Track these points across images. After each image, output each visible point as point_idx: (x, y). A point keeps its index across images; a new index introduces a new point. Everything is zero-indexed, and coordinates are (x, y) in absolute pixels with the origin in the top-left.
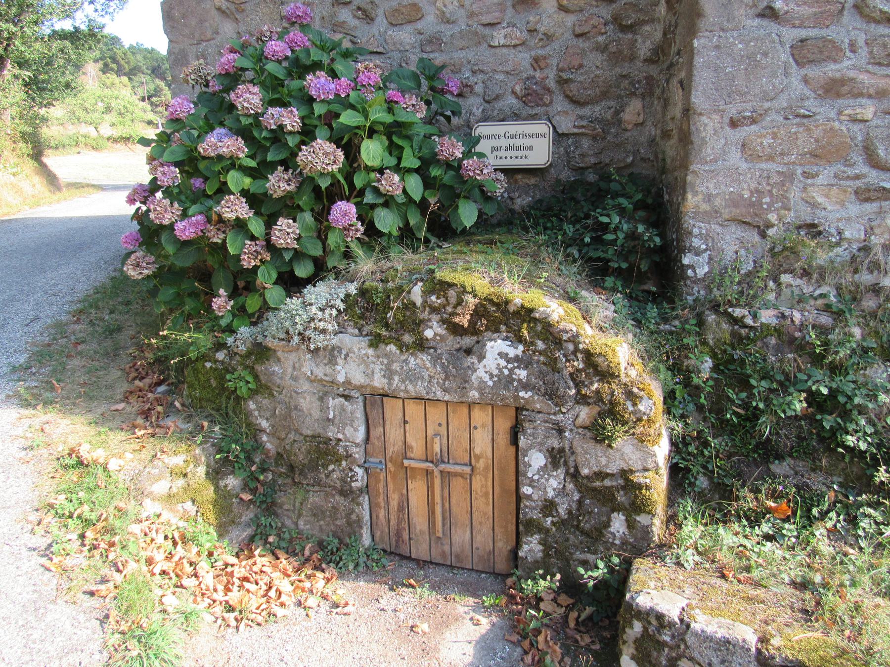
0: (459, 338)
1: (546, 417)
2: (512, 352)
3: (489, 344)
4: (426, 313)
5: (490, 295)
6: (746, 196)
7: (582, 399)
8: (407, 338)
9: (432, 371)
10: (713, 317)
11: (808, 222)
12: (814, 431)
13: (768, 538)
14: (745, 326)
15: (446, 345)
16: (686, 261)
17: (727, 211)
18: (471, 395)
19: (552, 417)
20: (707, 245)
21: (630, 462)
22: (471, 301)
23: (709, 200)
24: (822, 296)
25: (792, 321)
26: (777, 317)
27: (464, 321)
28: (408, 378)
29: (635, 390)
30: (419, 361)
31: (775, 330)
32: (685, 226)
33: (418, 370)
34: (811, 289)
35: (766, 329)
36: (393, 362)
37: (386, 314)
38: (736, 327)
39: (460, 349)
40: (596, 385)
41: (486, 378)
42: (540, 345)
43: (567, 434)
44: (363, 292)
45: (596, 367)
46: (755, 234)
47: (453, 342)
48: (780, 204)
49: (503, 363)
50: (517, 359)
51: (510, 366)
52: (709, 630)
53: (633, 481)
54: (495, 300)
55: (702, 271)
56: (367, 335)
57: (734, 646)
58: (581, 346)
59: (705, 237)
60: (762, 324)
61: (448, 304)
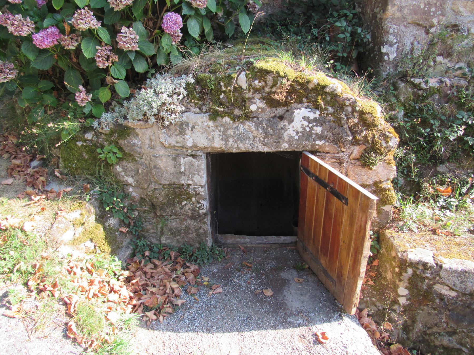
0: (274, 109)
1: (332, 155)
2: (312, 116)
3: (296, 112)
4: (251, 93)
5: (297, 78)
6: (422, 7)
7: (355, 142)
8: (237, 112)
9: (255, 133)
10: (403, 84)
11: (453, 23)
12: (460, 147)
13: (442, 208)
14: (421, 89)
15: (265, 114)
16: (384, 50)
17: (410, 17)
18: (283, 146)
19: (337, 155)
20: (397, 39)
21: (381, 177)
22: (286, 83)
23: (401, 10)
24: (460, 68)
25: (446, 84)
26: (438, 82)
27: (280, 97)
28: (239, 139)
29: (387, 134)
30: (246, 127)
31: (437, 90)
32: (385, 27)
33: (246, 133)
34: (453, 65)
35: (432, 92)
36: (228, 129)
37: (219, 95)
38: (416, 90)
39: (275, 116)
40: (364, 133)
41: (294, 134)
42: (330, 110)
43: (344, 164)
44: (198, 81)
45: (366, 121)
46: (423, 32)
47: (270, 112)
48: (440, 12)
49: (306, 123)
50: (315, 120)
51: (310, 125)
52: (454, 267)
53: (381, 187)
54: (301, 81)
55: (392, 57)
56: (206, 112)
57: (469, 273)
58: (357, 109)
59: (396, 35)
60: (430, 87)
61: (266, 85)
